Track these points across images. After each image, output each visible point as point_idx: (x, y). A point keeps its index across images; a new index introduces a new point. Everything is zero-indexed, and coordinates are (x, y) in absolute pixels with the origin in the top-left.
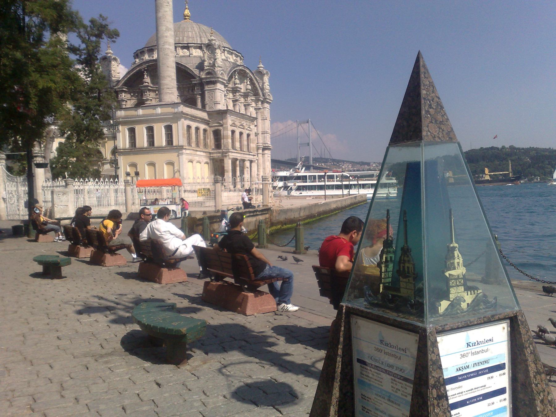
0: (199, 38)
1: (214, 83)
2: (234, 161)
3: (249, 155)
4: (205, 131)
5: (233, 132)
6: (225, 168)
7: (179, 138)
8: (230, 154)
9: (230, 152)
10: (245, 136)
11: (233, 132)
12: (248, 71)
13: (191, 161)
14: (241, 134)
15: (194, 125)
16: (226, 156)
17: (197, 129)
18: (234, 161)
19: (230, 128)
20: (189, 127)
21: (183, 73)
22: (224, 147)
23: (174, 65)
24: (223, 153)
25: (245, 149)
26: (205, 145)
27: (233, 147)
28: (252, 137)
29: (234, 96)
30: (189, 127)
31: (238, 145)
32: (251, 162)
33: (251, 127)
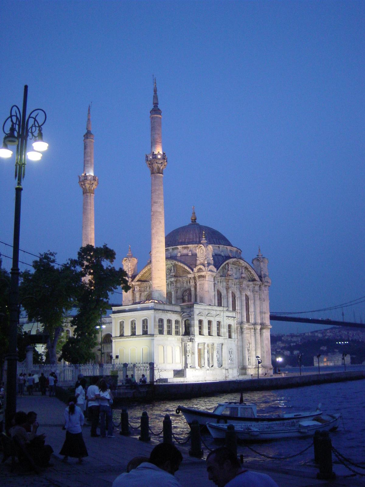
4: (177, 322)
11: (201, 322)
14: (210, 322)
17: (169, 321)
20: (161, 321)
29: (227, 284)
31: (205, 331)
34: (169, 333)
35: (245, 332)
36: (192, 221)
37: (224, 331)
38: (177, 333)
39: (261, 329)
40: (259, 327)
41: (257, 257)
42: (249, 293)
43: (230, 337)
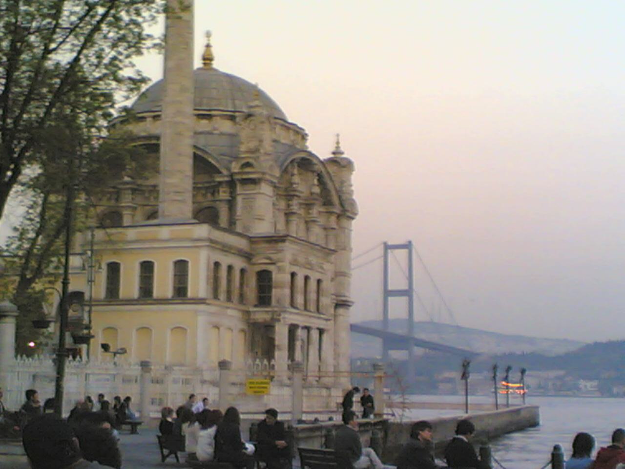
0: (230, 102)
1: (254, 182)
3: (319, 318)
4: (243, 271)
5: (293, 275)
6: (277, 343)
7: (198, 283)
8: (286, 315)
9: (285, 312)
10: (313, 285)
11: (293, 275)
12: (315, 161)
13: (217, 327)
14: (307, 278)
15: (226, 260)
16: (279, 320)
17: (230, 268)
18: (293, 329)
19: (290, 269)
20: (217, 264)
21: (202, 164)
22: (278, 301)
23: (190, 151)
24: (273, 312)
25: (312, 307)
26: (242, 298)
27: (293, 304)
28: (326, 284)
29: (289, 206)
30: (217, 264)
31: (300, 299)
32: (321, 332)
33: (325, 267)
36: (205, 64)
41: (332, 156)
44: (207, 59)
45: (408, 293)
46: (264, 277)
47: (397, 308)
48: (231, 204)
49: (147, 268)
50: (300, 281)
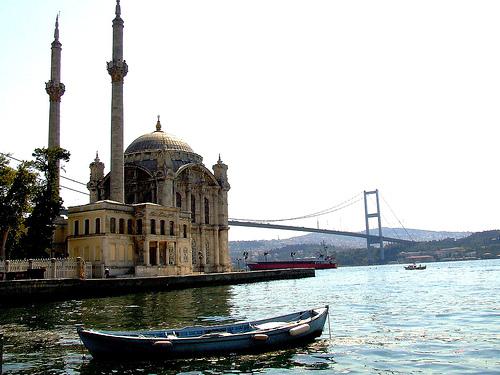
2: (154, 244)
4: (130, 221)
5: (153, 221)
7: (103, 228)
11: (153, 221)
14: (163, 222)
20: (113, 220)
27: (153, 232)
30: (113, 220)
31: (158, 230)
34: (122, 232)
35: (204, 232)
37: (176, 230)
38: (130, 232)
39: (220, 230)
40: (217, 228)
42: (208, 197)
43: (185, 236)
44: (159, 127)
45: (377, 215)
46: (140, 222)
47: (373, 223)
48: (155, 189)
49: (87, 221)
50: (158, 223)
